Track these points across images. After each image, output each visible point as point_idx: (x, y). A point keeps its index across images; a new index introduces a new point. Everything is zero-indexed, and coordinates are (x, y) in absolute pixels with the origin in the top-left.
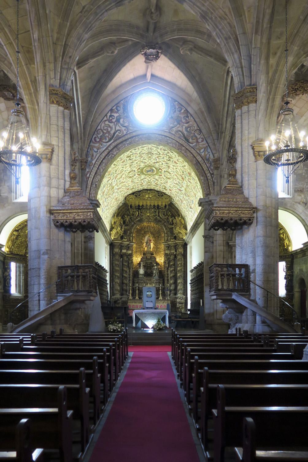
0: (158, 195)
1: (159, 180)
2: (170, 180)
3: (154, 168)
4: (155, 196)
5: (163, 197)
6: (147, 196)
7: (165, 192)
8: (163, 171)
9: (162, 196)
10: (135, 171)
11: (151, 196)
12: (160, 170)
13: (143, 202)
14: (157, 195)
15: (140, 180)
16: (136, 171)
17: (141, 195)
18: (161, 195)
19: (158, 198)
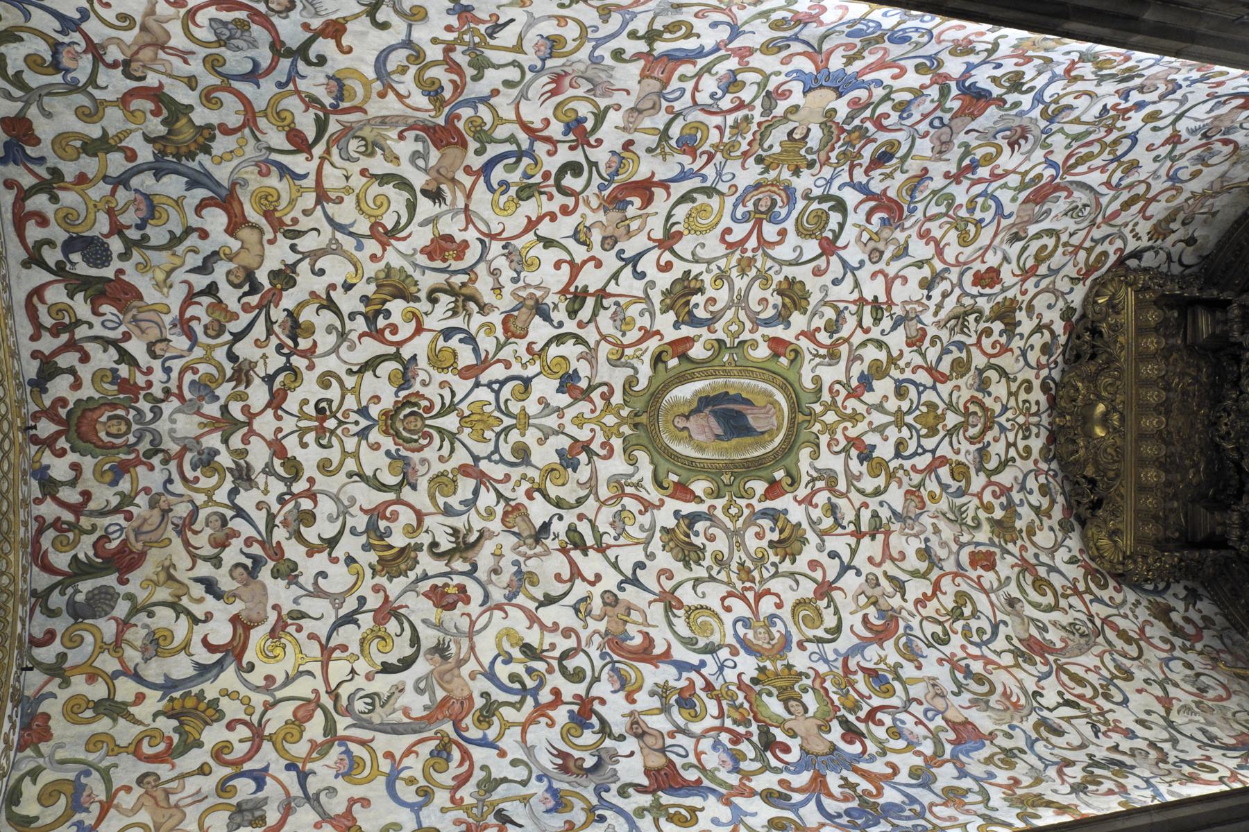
0: (1093, 357)
1: (871, 353)
2: (813, 284)
3: (685, 392)
4: (1092, 379)
5: (1104, 327)
6: (1099, 432)
7: (1053, 317)
8: (686, 331)
9: (1096, 332)
10: (693, 518)
11: (1101, 408)
12: (697, 352)
13: (1142, 462)
14: (1092, 368)
15: (868, 484)
16: (688, 508)
17: (1090, 471)
18: (1087, 336)
19: (1111, 360)
